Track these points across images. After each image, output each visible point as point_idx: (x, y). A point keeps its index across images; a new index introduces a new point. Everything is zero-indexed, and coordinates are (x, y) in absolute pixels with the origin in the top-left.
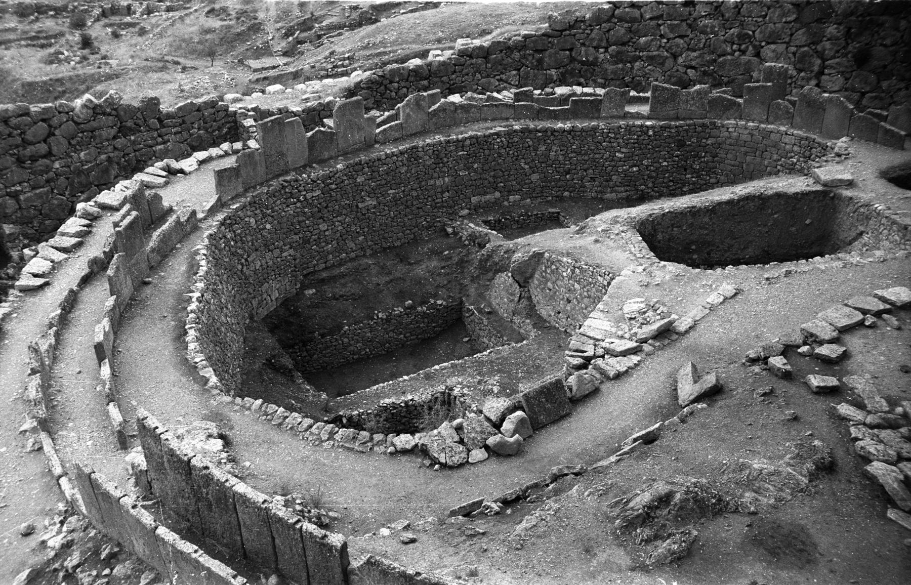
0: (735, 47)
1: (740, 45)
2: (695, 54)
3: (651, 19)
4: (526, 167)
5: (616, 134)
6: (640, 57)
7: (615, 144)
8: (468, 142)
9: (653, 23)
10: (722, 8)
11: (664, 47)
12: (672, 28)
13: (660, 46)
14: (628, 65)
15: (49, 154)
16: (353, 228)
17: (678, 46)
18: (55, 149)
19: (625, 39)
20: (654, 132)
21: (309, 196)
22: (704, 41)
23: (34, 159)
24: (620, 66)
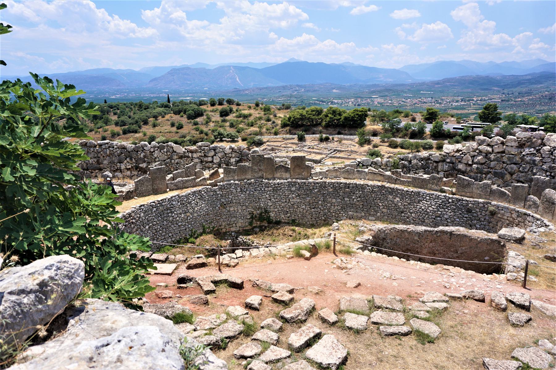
0: (548, 173)
1: (551, 173)
2: (523, 174)
3: (498, 153)
4: (380, 204)
5: (430, 198)
6: (491, 172)
7: (429, 203)
8: (351, 185)
9: (499, 155)
10: (541, 151)
11: (505, 168)
12: (509, 159)
13: (502, 168)
14: (484, 175)
15: (212, 162)
16: (285, 209)
17: (511, 168)
18: (215, 161)
19: (483, 162)
20: (453, 202)
21: (266, 189)
22: (528, 167)
23: (207, 162)
24: (479, 175)
